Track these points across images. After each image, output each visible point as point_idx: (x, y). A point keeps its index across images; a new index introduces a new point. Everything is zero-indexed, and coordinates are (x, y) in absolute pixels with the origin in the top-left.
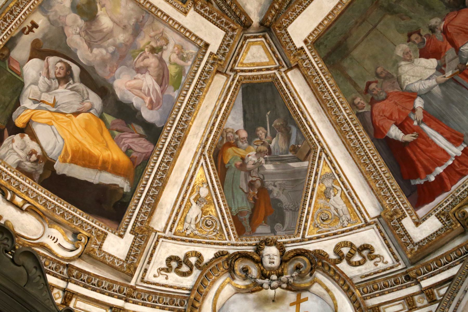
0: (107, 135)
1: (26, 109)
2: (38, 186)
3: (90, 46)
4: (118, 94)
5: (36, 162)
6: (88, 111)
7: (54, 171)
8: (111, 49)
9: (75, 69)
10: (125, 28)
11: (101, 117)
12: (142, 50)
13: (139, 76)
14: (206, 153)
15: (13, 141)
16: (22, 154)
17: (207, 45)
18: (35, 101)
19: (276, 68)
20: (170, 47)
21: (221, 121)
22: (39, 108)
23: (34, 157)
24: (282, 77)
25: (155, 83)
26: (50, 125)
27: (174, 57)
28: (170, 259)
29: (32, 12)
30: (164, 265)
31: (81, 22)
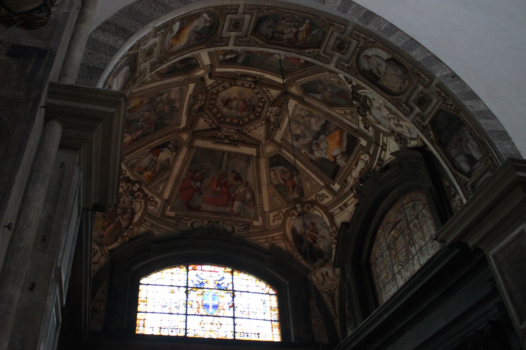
0: (332, 135)
1: (329, 158)
2: (350, 157)
3: (307, 137)
4: (319, 130)
5: (344, 156)
6: (326, 139)
7: (345, 152)
8: (306, 130)
9: (315, 142)
10: (299, 126)
11: (327, 135)
12: (304, 121)
13: (312, 123)
14: (330, 108)
15: (338, 162)
16: (342, 160)
17: (296, 104)
18: (326, 155)
19: (296, 85)
20: (301, 113)
21: (319, 101)
22: (328, 153)
23: (342, 157)
24: (298, 84)
25: (313, 118)
26: (332, 151)
27: (303, 112)
28: (365, 129)
29: (301, 153)
30: (367, 130)
31: (301, 139)
